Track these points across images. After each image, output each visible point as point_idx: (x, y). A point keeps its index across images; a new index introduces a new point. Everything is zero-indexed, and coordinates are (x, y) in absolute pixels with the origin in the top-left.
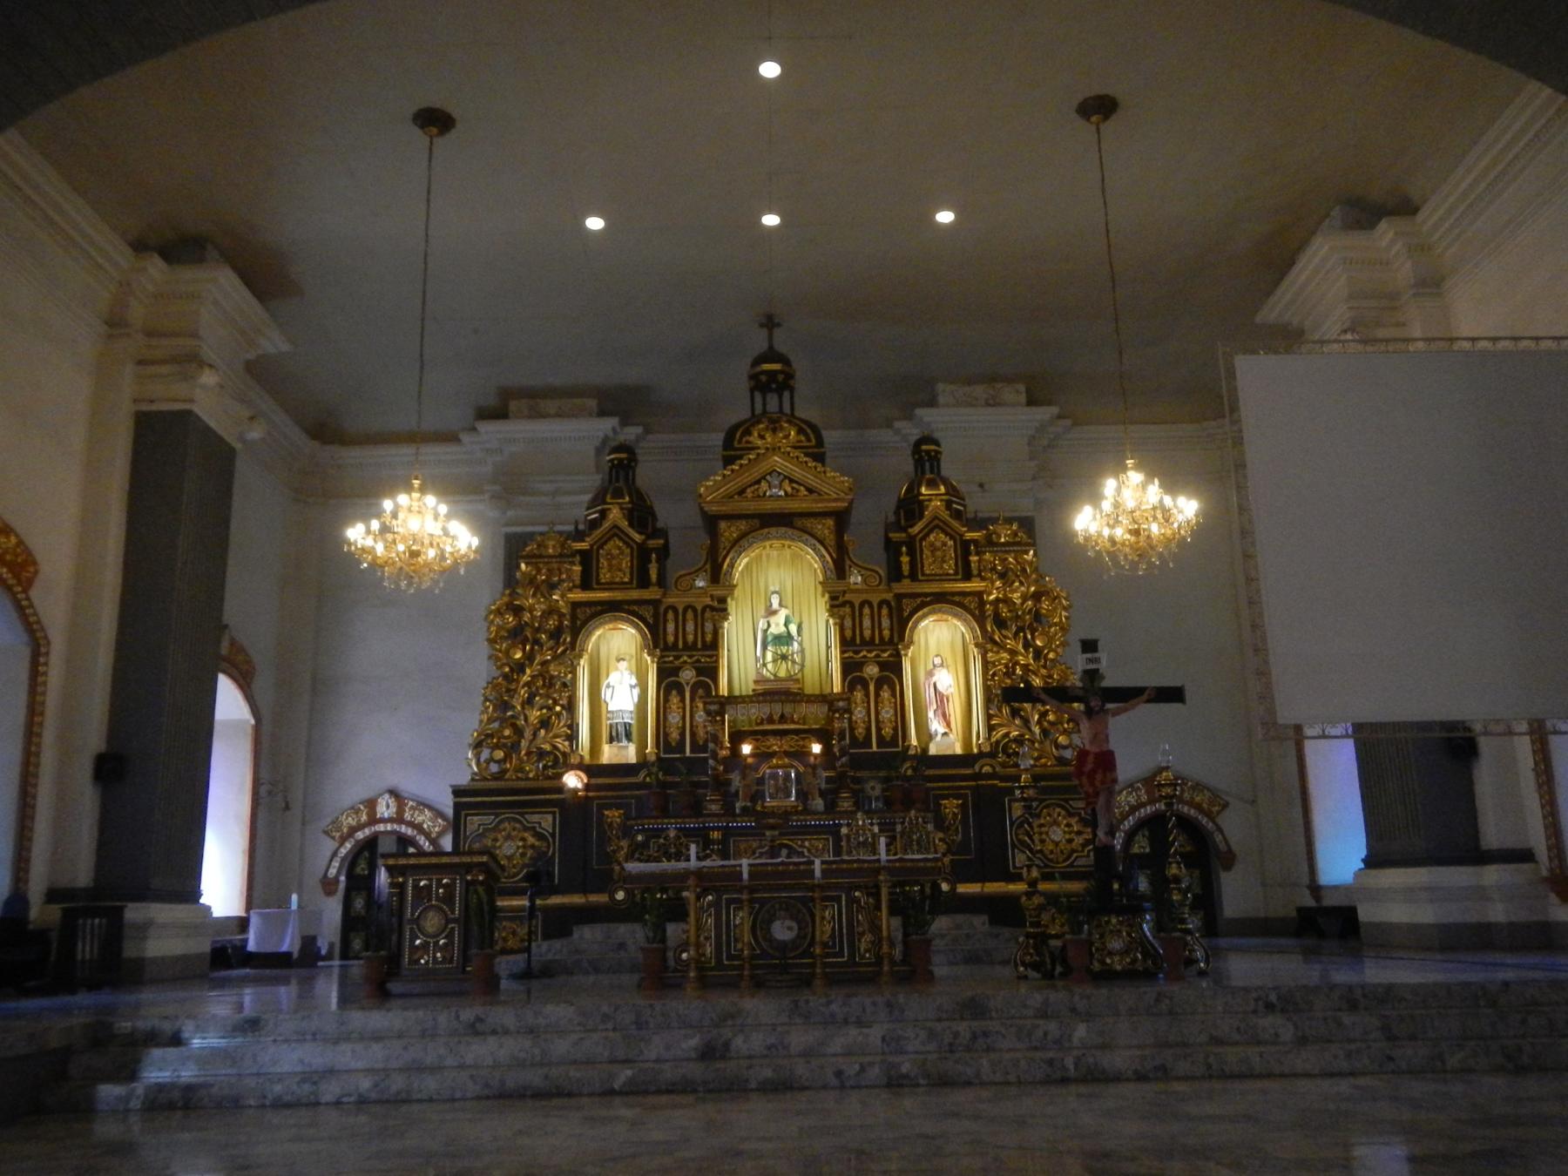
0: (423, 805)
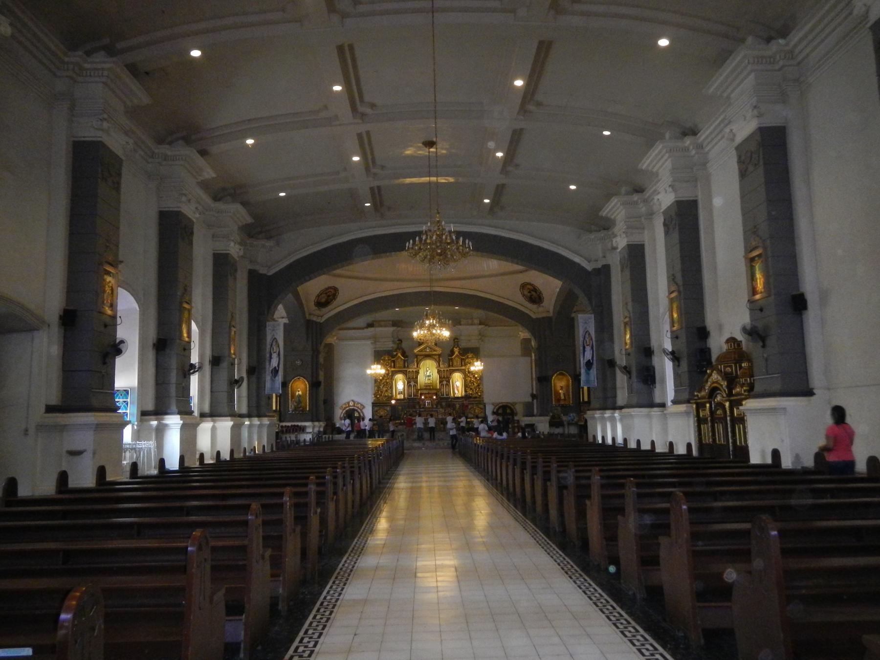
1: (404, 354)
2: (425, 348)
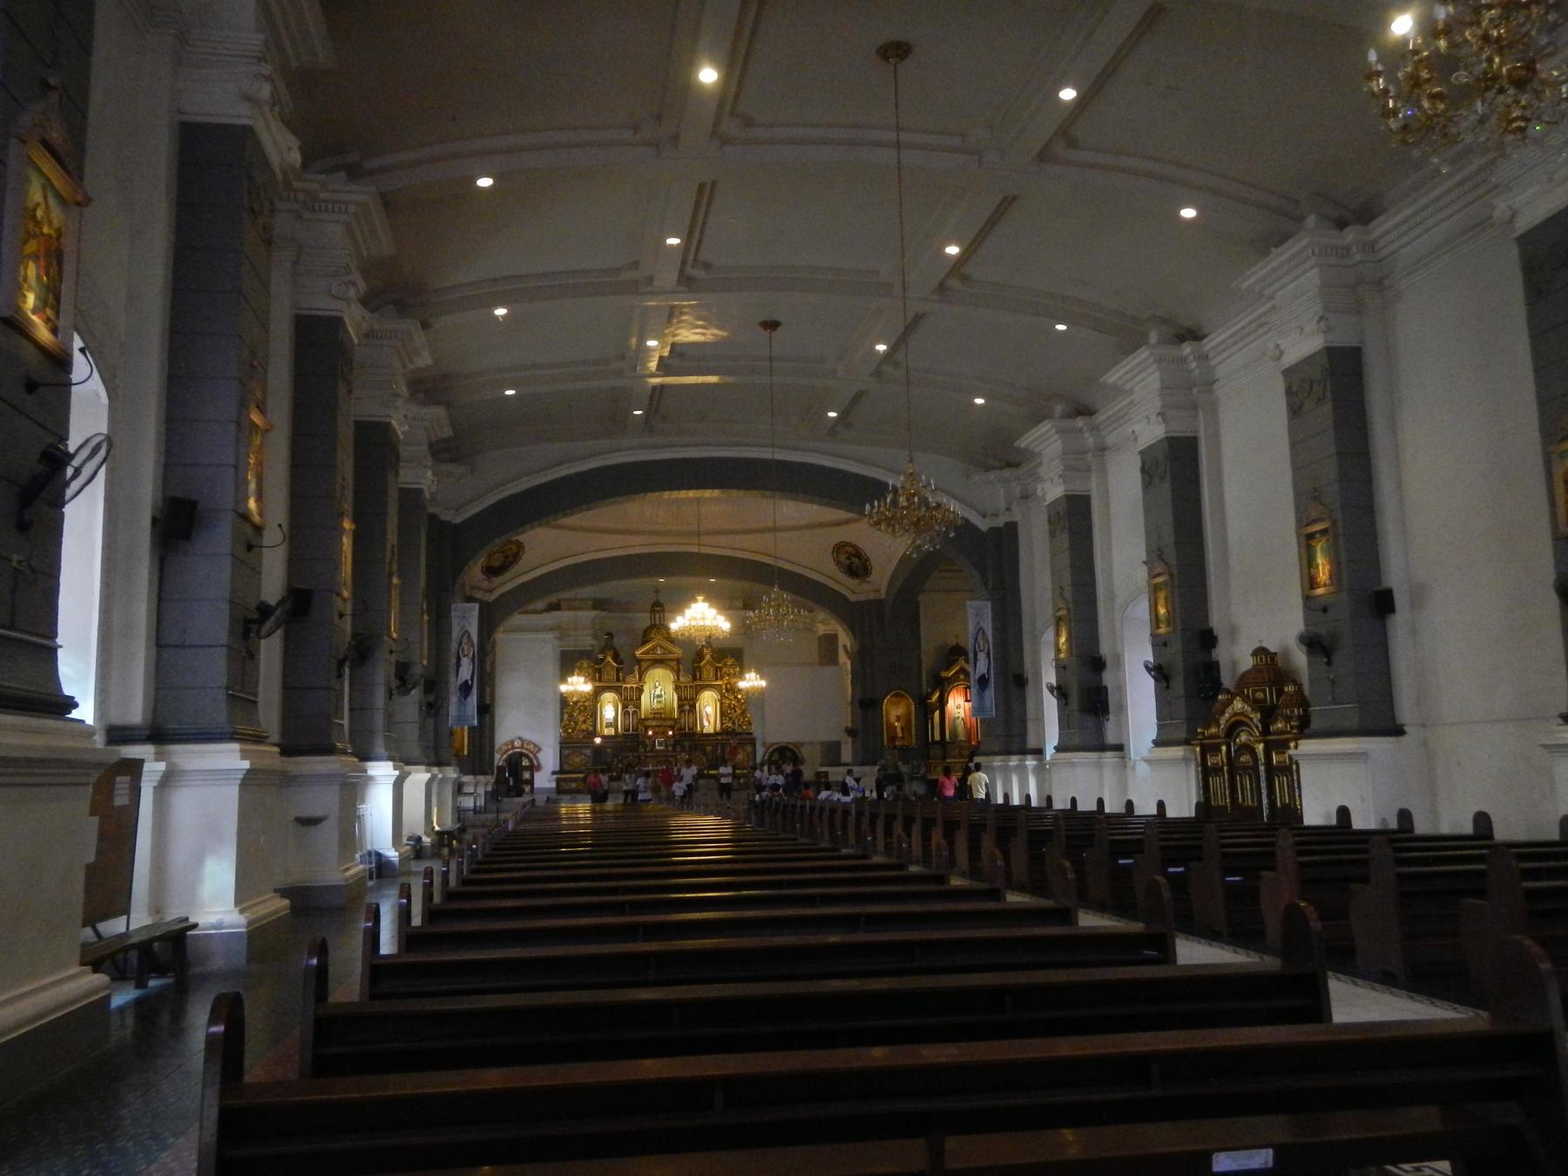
0: (530, 743)
1: (616, 658)
2: (654, 649)
